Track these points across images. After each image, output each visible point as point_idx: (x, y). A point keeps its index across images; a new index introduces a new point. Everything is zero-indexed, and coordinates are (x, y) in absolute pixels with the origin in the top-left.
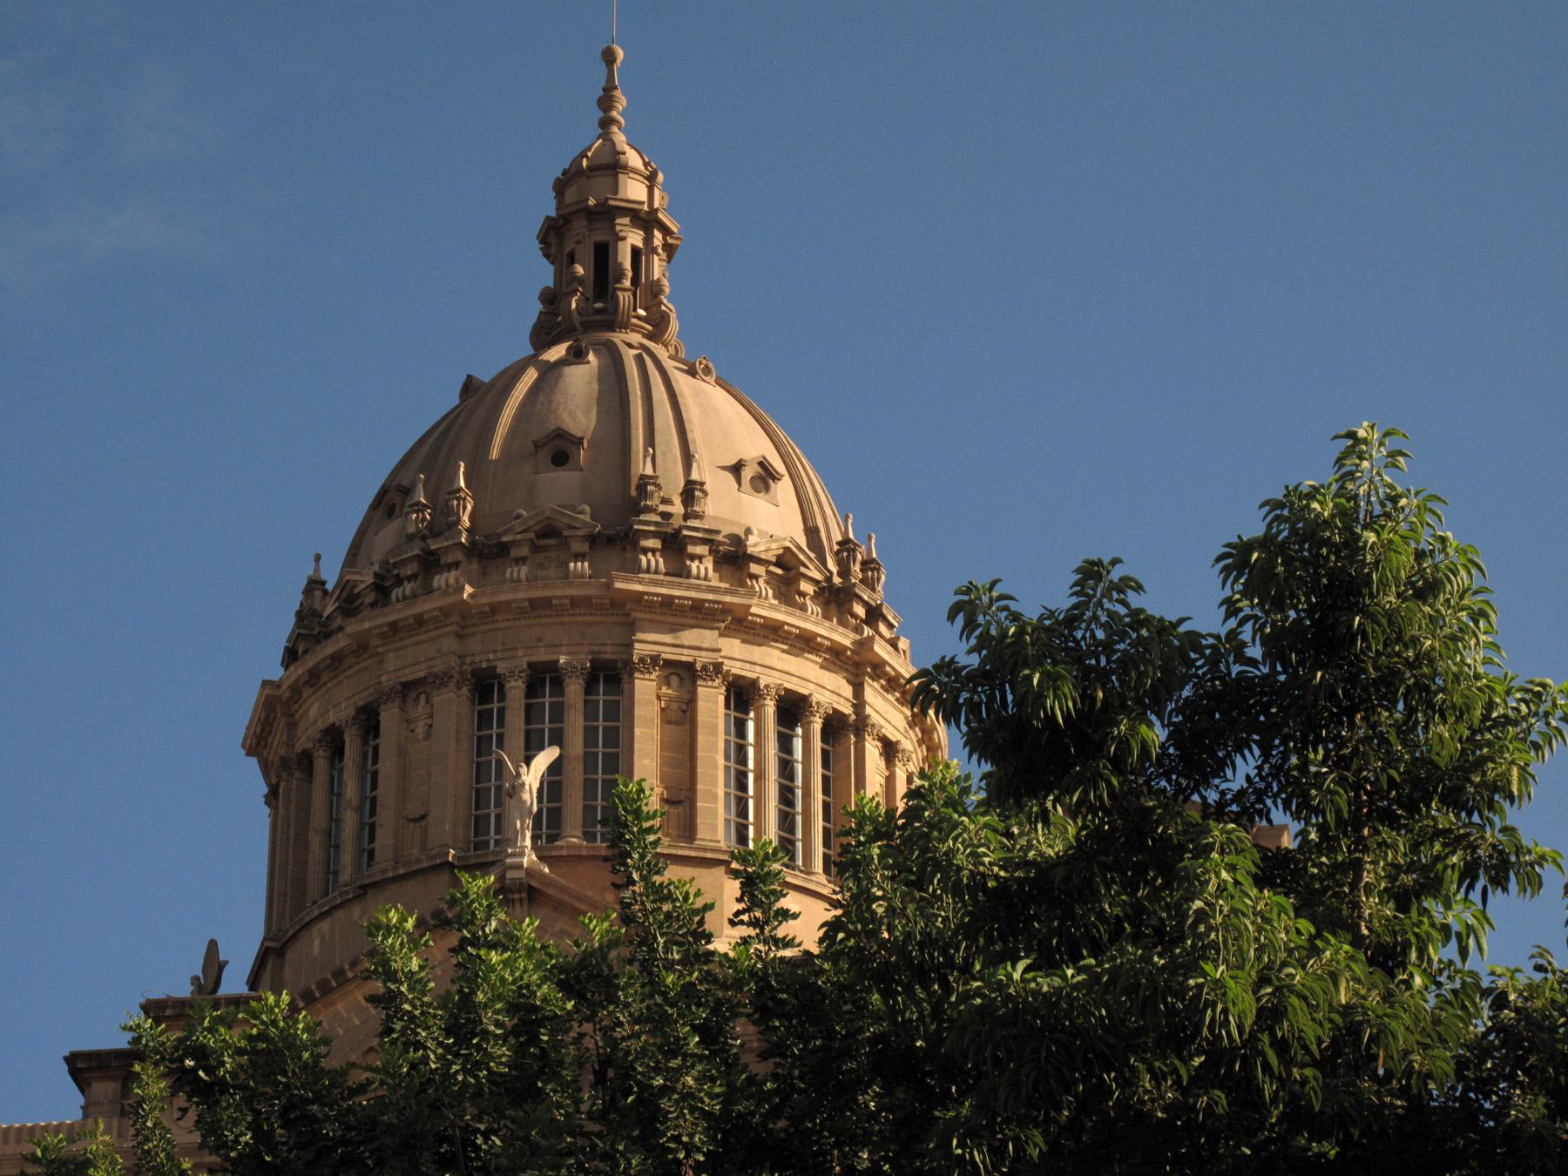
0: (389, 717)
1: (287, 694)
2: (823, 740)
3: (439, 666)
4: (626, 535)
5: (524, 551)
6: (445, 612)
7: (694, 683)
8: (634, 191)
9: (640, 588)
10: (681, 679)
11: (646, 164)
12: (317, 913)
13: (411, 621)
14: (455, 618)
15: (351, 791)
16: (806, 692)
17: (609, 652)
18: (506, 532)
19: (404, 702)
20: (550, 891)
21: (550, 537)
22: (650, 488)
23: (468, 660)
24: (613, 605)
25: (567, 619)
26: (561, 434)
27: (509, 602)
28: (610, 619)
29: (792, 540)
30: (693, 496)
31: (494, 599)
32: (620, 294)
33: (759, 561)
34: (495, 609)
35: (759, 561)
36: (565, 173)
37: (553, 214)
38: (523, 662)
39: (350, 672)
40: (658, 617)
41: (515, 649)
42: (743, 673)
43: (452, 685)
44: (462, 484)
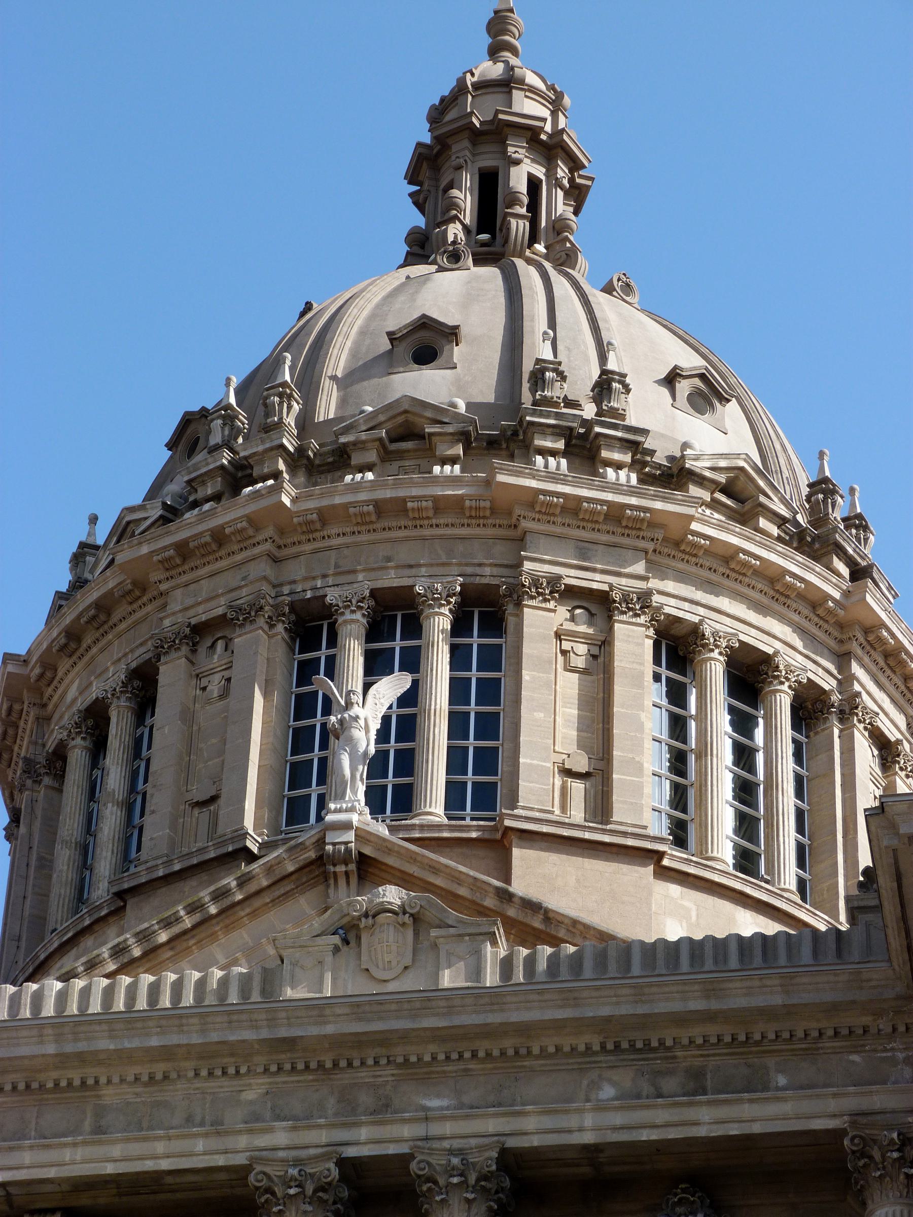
0: (172, 675)
1: (37, 671)
2: (796, 726)
3: (244, 597)
4: (515, 433)
5: (372, 456)
6: (253, 522)
7: (610, 619)
8: (528, 107)
9: (534, 484)
10: (592, 615)
11: (552, 88)
12: (56, 945)
13: (208, 539)
14: (270, 532)
15: (115, 777)
16: (770, 651)
17: (488, 575)
18: (346, 430)
19: (194, 651)
20: (391, 861)
21: (409, 435)
22: (549, 375)
23: (286, 590)
24: (493, 511)
25: (427, 532)
26: (425, 324)
27: (346, 506)
28: (490, 531)
29: (748, 459)
30: (610, 389)
31: (325, 502)
32: (513, 222)
33: (701, 481)
34: (325, 517)
35: (701, 481)
36: (443, 100)
37: (427, 139)
38: (364, 584)
39: (123, 626)
40: (558, 530)
41: (354, 572)
42: (681, 614)
43: (261, 622)
44: (287, 377)
